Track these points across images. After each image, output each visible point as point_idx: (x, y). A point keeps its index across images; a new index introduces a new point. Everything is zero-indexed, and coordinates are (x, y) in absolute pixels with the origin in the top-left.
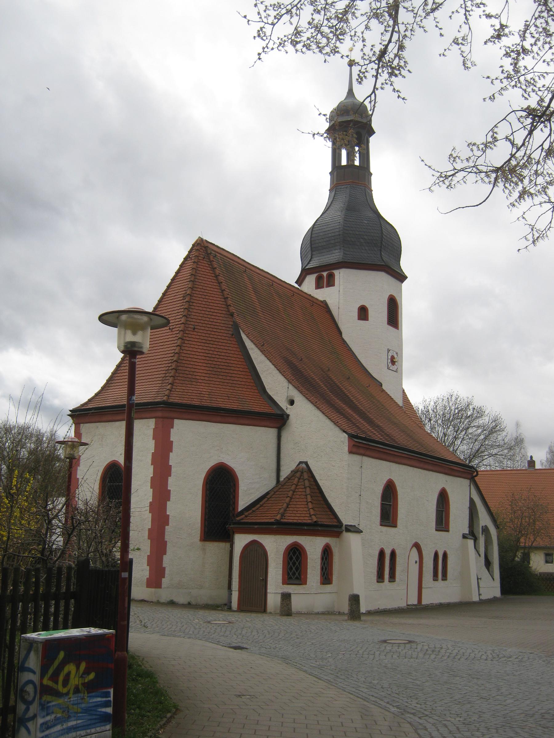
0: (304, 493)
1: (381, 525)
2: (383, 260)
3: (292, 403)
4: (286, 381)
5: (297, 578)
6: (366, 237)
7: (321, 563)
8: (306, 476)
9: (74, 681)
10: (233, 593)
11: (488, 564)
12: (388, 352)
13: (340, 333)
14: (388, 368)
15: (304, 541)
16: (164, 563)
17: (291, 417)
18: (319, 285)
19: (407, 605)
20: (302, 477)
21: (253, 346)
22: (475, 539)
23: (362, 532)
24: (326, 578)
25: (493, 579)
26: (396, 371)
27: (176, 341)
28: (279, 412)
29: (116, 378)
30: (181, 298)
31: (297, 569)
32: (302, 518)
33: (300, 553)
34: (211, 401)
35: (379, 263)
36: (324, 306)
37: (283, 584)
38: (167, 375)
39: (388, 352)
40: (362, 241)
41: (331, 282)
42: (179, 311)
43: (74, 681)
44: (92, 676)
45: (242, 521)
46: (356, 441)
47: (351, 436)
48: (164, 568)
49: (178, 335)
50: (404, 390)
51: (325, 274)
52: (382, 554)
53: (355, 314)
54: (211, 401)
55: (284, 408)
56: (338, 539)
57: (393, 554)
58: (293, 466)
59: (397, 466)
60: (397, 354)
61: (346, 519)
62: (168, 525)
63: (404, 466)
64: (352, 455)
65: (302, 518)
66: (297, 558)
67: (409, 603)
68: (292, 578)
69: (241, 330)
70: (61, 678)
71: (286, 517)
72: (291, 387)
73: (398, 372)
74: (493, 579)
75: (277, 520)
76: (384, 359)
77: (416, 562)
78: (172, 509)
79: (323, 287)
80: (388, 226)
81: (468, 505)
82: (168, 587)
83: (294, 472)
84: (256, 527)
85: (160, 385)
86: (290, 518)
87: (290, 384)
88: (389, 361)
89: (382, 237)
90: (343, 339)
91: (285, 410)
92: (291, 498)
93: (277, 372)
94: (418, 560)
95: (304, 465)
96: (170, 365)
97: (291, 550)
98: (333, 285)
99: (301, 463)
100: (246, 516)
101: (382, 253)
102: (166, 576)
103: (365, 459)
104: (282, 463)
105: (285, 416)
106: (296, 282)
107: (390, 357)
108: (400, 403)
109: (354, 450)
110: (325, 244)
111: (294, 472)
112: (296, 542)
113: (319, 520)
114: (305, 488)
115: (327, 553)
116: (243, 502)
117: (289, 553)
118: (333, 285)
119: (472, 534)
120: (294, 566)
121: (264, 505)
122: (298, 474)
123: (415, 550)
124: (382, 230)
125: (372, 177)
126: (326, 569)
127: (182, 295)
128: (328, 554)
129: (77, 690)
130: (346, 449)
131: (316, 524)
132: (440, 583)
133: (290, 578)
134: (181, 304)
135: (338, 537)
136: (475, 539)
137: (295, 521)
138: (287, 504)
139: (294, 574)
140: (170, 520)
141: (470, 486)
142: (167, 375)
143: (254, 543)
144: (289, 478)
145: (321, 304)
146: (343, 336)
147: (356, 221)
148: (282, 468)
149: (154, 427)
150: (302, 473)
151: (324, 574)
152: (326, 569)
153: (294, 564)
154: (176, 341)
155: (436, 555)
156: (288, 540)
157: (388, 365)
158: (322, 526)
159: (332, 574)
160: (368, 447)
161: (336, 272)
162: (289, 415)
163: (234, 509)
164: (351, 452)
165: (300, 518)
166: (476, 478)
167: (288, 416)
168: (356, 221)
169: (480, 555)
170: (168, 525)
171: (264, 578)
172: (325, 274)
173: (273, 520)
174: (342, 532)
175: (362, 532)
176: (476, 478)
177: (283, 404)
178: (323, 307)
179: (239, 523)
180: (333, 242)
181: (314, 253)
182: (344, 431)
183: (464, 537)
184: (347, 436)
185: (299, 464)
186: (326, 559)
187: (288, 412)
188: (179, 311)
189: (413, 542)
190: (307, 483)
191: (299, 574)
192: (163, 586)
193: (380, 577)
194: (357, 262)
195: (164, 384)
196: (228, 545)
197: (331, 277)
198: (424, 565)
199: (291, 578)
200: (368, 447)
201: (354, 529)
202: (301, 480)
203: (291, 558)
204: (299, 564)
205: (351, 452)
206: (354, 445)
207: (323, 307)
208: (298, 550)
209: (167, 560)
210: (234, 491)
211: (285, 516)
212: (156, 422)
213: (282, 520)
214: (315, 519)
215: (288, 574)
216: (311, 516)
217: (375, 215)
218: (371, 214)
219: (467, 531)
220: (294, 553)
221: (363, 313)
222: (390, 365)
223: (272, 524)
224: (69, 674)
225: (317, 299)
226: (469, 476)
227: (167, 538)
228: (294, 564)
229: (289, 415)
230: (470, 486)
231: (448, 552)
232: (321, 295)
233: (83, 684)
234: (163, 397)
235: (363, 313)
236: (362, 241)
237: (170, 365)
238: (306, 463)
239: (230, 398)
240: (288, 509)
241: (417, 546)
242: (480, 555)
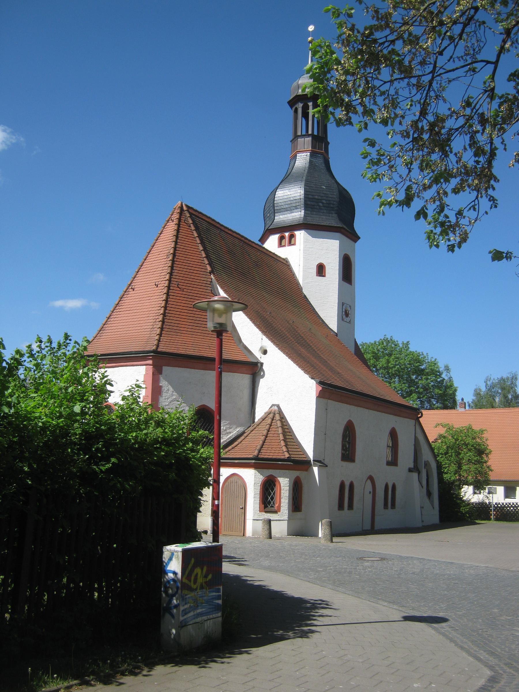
3: (265, 352)
6: (324, 201)
8: (277, 417)
9: (200, 580)
11: (429, 494)
12: (343, 306)
18: (280, 245)
19: (363, 530)
22: (419, 473)
25: (433, 508)
26: (350, 322)
27: (161, 296)
29: (107, 329)
30: (165, 257)
32: (277, 454)
34: (194, 351)
35: (335, 225)
36: (285, 263)
38: (155, 326)
39: (343, 306)
40: (321, 204)
42: (164, 268)
43: (200, 580)
44: (210, 577)
49: (163, 290)
50: (355, 339)
51: (287, 234)
52: (342, 485)
53: (314, 270)
54: (194, 351)
55: (259, 357)
57: (352, 485)
58: (266, 409)
59: (356, 408)
60: (350, 307)
63: (362, 409)
65: (277, 454)
67: (364, 529)
70: (193, 578)
71: (262, 454)
74: (433, 508)
77: (370, 492)
81: (414, 443)
83: (269, 413)
85: (148, 336)
88: (344, 313)
91: (259, 359)
94: (371, 490)
95: (276, 408)
96: (157, 317)
99: (273, 405)
105: (259, 364)
106: (259, 241)
107: (344, 310)
110: (287, 206)
111: (267, 414)
112: (271, 475)
113: (292, 456)
119: (415, 469)
121: (242, 443)
122: (271, 416)
123: (369, 482)
125: (329, 146)
126: (296, 498)
127: (166, 254)
129: (202, 587)
131: (289, 460)
132: (390, 511)
133: (266, 507)
134: (165, 263)
135: (307, 470)
136: (419, 473)
137: (270, 457)
141: (415, 425)
142: (155, 326)
149: (144, 373)
152: (296, 498)
154: (161, 296)
155: (387, 486)
157: (342, 317)
166: (420, 419)
169: (422, 487)
171: (243, 506)
172: (287, 234)
176: (420, 419)
180: (294, 205)
183: (410, 470)
185: (271, 407)
186: (297, 490)
188: (164, 268)
189: (368, 476)
193: (341, 507)
194: (316, 223)
195: (153, 335)
197: (292, 236)
198: (377, 495)
204: (274, 494)
211: (261, 453)
212: (146, 369)
214: (287, 455)
219: (412, 465)
221: (321, 270)
222: (344, 317)
224: (197, 575)
225: (280, 257)
230: (415, 425)
231: (396, 484)
232: (283, 253)
233: (206, 582)
234: (152, 347)
235: (321, 270)
236: (321, 204)
237: (157, 317)
238: (278, 406)
239: (211, 348)
241: (371, 478)
242: (422, 487)
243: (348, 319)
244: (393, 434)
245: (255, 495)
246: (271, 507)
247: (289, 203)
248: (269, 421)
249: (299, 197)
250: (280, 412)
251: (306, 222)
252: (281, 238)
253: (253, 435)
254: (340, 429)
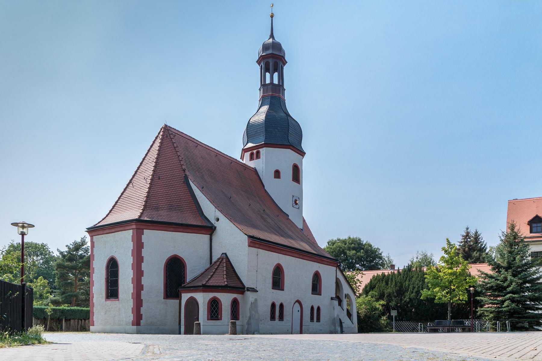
0: (222, 270)
1: (272, 289)
2: (289, 142)
3: (218, 220)
4: (214, 207)
5: (216, 317)
7: (231, 309)
8: (224, 261)
10: (181, 326)
13: (264, 186)
14: (293, 206)
15: (220, 296)
16: (141, 311)
17: (217, 228)
18: (251, 158)
20: (222, 262)
21: (196, 188)
23: (258, 291)
24: (235, 317)
28: (210, 225)
31: (216, 312)
33: (218, 303)
36: (255, 171)
37: (208, 320)
41: (258, 156)
45: (186, 286)
46: (252, 240)
47: (250, 237)
48: (142, 315)
51: (255, 151)
56: (242, 295)
58: (219, 256)
61: (247, 284)
62: (143, 290)
64: (250, 248)
65: (219, 283)
66: (216, 306)
68: (213, 317)
69: (189, 179)
72: (217, 210)
73: (300, 208)
75: (203, 284)
76: (291, 202)
78: (145, 281)
79: (254, 160)
80: (293, 122)
82: (144, 325)
83: (219, 259)
84: (192, 289)
86: (212, 283)
87: (216, 209)
89: (289, 128)
90: (265, 190)
91: (214, 224)
92: (214, 273)
93: (209, 202)
95: (224, 255)
97: (213, 301)
98: (260, 158)
99: (223, 254)
100: (188, 284)
101: (289, 138)
102: (143, 319)
103: (259, 250)
104: (213, 254)
105: (213, 228)
108: (300, 226)
109: (252, 245)
114: (223, 267)
115: (235, 304)
116: (189, 277)
117: (211, 303)
118: (260, 158)
120: (214, 310)
122: (220, 260)
124: (289, 123)
126: (235, 312)
128: (236, 304)
130: (247, 244)
131: (226, 286)
138: (211, 276)
139: (214, 314)
140: (144, 287)
143: (192, 298)
144: (215, 263)
145: (252, 169)
146: (265, 188)
147: (273, 118)
148: (213, 258)
150: (223, 259)
151: (234, 315)
152: (235, 312)
153: (214, 309)
156: (211, 295)
158: (230, 287)
159: (239, 315)
160: (261, 243)
161: (260, 150)
162: (216, 227)
163: (184, 281)
164: (249, 246)
165: (218, 283)
167: (215, 227)
168: (273, 118)
170: (143, 290)
172: (255, 151)
173: (201, 285)
174: (245, 291)
175: (258, 291)
177: (213, 221)
178: (254, 171)
179: (184, 287)
181: (249, 139)
182: (245, 234)
184: (247, 236)
185: (222, 255)
187: (215, 225)
190: (225, 265)
191: (218, 314)
192: (141, 325)
196: (178, 301)
197: (258, 153)
199: (213, 317)
200: (261, 243)
201: (254, 290)
202: (222, 263)
203: (213, 306)
204: (217, 309)
205: (249, 246)
206: (251, 242)
207: (254, 171)
208: (216, 301)
209: (143, 310)
210: (184, 271)
213: (206, 284)
214: (226, 283)
215: (211, 314)
216: (224, 282)
217: (285, 115)
218: (283, 115)
220: (214, 303)
221: (277, 174)
223: (200, 286)
226: (336, 265)
227: (142, 298)
228: (214, 309)
229: (216, 227)
232: (252, 164)
235: (277, 174)
238: (226, 254)
240: (211, 279)
243: (297, 206)
244: (317, 277)
245: (203, 309)
246: (215, 317)
247: (256, 130)
248: (218, 264)
249: (262, 126)
250: (227, 257)
251: (266, 142)
252: (252, 154)
253: (207, 272)
254: (271, 269)
